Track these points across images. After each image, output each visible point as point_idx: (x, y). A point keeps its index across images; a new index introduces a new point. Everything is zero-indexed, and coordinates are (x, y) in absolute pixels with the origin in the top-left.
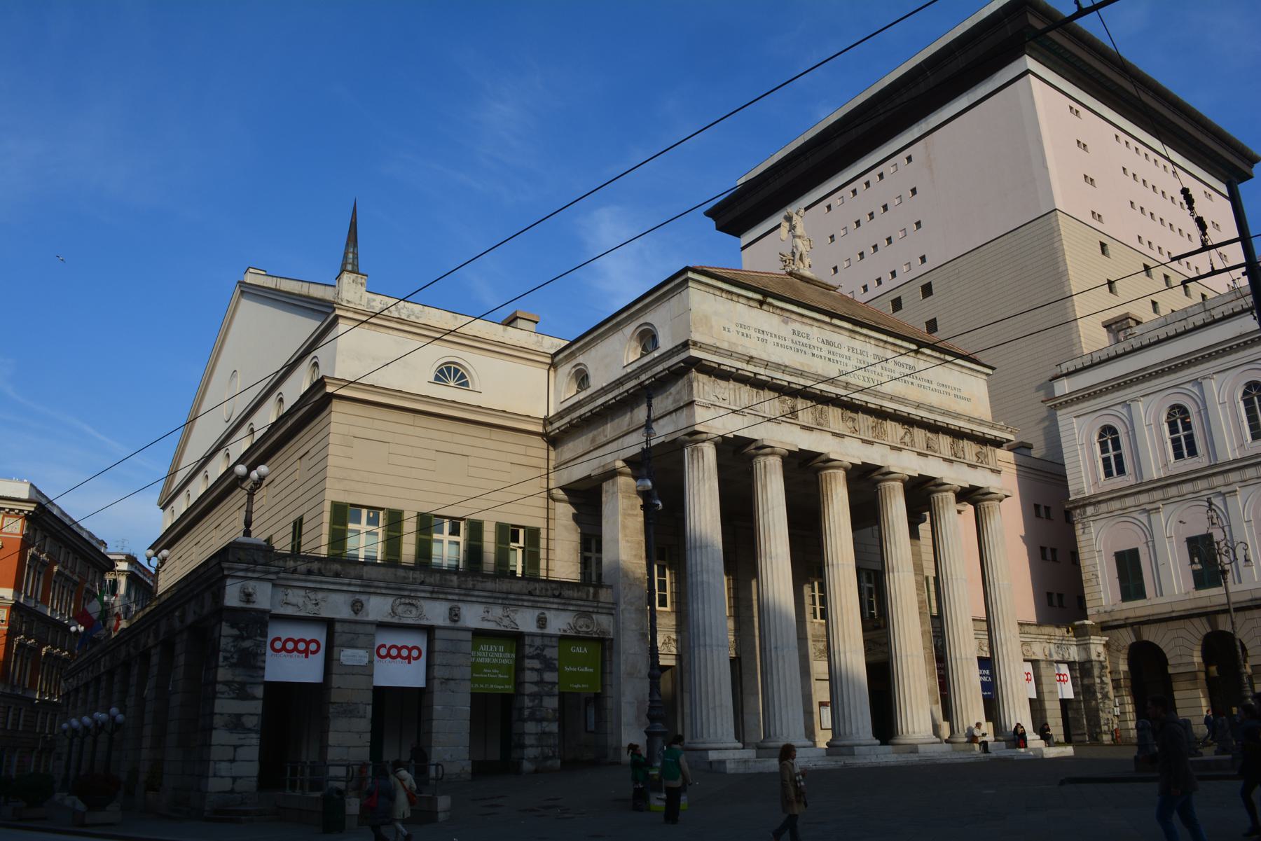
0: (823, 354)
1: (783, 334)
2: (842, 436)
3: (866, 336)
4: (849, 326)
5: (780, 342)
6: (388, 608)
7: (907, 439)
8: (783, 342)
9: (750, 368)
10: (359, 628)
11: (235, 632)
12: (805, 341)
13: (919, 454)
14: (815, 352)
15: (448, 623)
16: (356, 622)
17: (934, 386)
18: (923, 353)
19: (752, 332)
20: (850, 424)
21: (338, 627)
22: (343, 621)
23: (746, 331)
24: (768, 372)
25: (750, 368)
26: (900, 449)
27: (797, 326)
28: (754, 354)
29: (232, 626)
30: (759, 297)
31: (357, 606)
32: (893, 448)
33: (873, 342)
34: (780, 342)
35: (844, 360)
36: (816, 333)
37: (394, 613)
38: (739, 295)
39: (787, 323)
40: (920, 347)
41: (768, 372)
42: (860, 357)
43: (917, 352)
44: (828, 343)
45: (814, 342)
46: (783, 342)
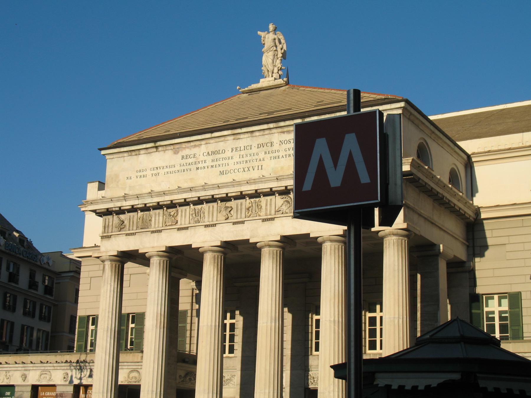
0: (205, 165)
2: (214, 225)
5: (168, 170)
6: (37, 377)
10: (24, 389)
12: (190, 161)
14: (200, 165)
15: (63, 383)
19: (149, 173)
20: (224, 213)
21: (17, 389)
22: (18, 386)
23: (141, 174)
26: (273, 219)
27: (186, 152)
32: (264, 220)
33: (257, 134)
34: (168, 170)
39: (178, 152)
42: (242, 153)
44: (214, 153)
45: (202, 158)
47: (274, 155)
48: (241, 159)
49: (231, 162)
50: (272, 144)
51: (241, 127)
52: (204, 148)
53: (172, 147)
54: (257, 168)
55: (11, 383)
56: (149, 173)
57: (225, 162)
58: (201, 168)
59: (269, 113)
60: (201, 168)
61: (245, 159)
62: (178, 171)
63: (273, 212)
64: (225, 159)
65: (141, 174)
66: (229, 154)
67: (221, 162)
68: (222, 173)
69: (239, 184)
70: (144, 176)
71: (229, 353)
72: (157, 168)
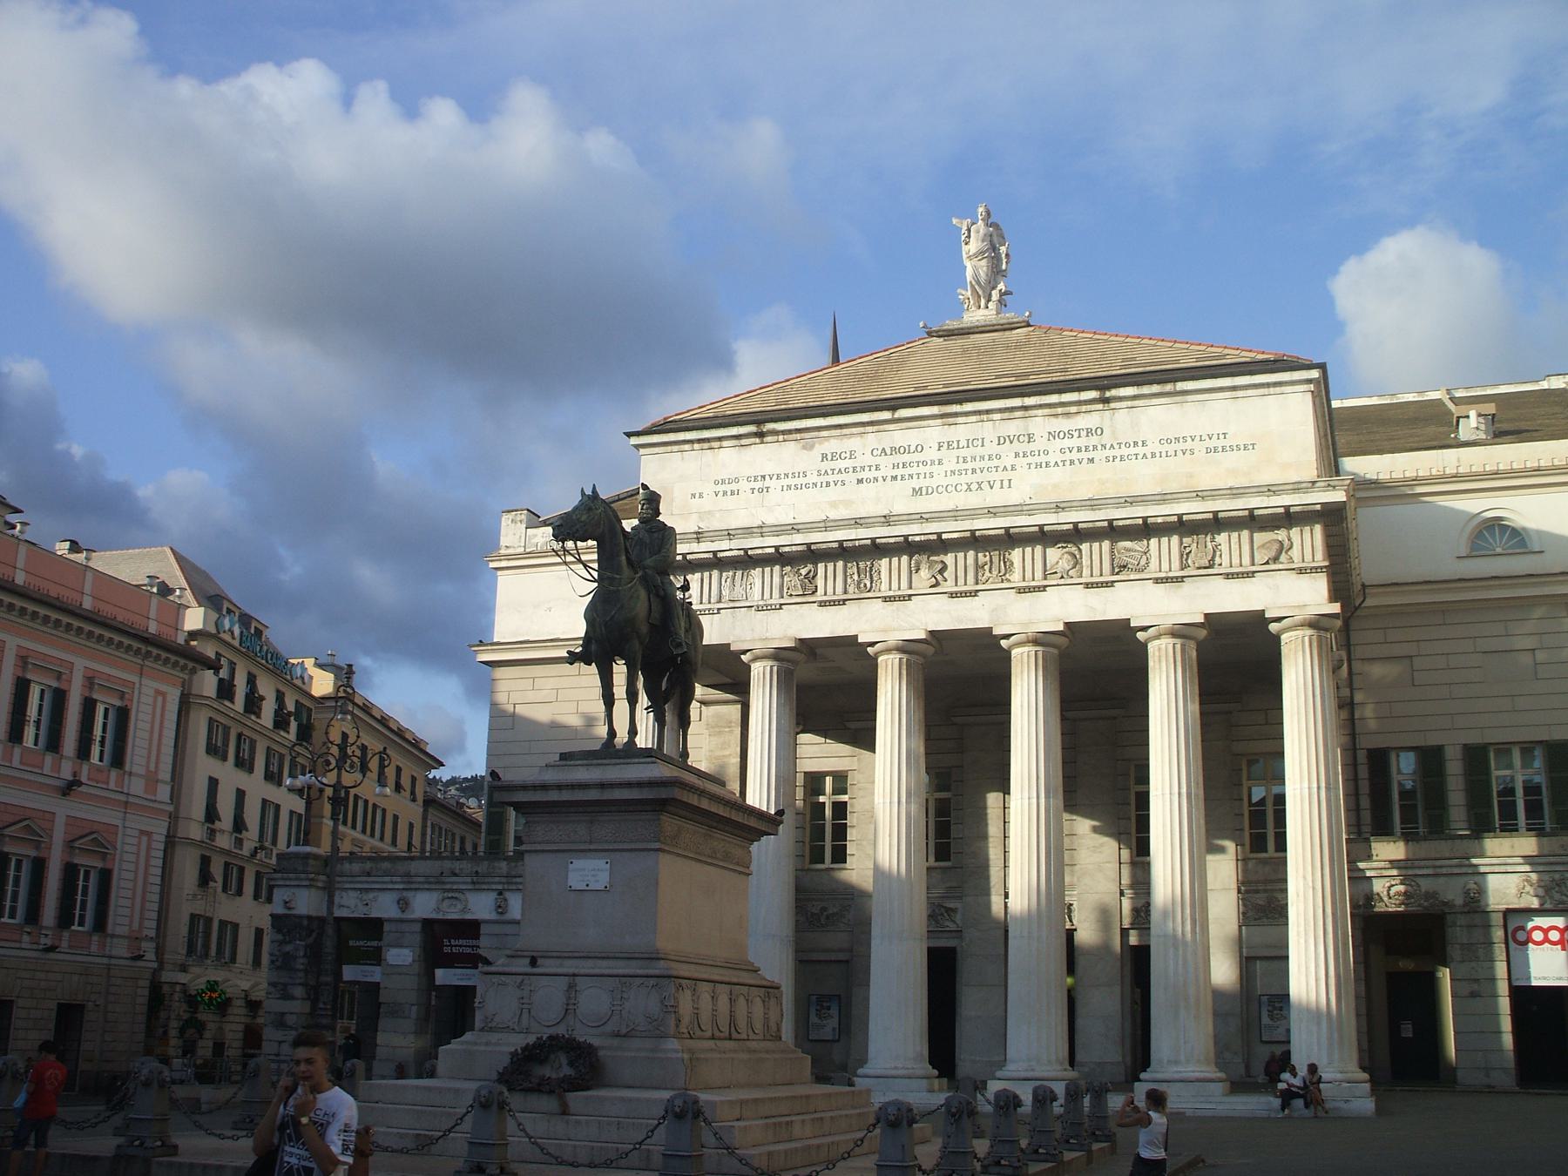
0: (878, 474)
1: (799, 468)
3: (979, 412)
4: (935, 410)
7: (1065, 564)
8: (802, 480)
9: (704, 546)
11: (280, 937)
13: (1088, 586)
16: (402, 921)
17: (1153, 446)
18: (1121, 399)
19: (744, 486)
21: (387, 927)
22: (390, 920)
23: (728, 488)
24: (735, 544)
25: (704, 546)
27: (832, 445)
28: (704, 526)
29: (279, 931)
30: (752, 428)
31: (404, 904)
32: (1021, 590)
33: (997, 416)
35: (928, 469)
36: (863, 444)
37: (438, 910)
38: (720, 439)
39: (812, 447)
40: (1103, 389)
41: (735, 544)
43: (1106, 401)
45: (869, 460)
46: (802, 480)
47: (1037, 459)
48: (962, 466)
49: (935, 469)
50: (1030, 438)
51: (960, 402)
52: (872, 439)
53: (798, 436)
54: (998, 485)
55: (374, 914)
56: (744, 486)
57: (922, 469)
58: (868, 481)
59: (1017, 376)
60: (868, 481)
61: (970, 465)
62: (815, 485)
63: (1039, 574)
64: (924, 463)
65: (728, 488)
66: (931, 454)
67: (914, 470)
68: (917, 492)
69: (973, 513)
70: (732, 493)
71: (833, 862)
72: (763, 477)
